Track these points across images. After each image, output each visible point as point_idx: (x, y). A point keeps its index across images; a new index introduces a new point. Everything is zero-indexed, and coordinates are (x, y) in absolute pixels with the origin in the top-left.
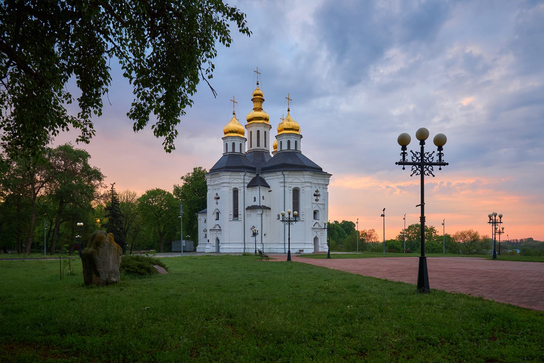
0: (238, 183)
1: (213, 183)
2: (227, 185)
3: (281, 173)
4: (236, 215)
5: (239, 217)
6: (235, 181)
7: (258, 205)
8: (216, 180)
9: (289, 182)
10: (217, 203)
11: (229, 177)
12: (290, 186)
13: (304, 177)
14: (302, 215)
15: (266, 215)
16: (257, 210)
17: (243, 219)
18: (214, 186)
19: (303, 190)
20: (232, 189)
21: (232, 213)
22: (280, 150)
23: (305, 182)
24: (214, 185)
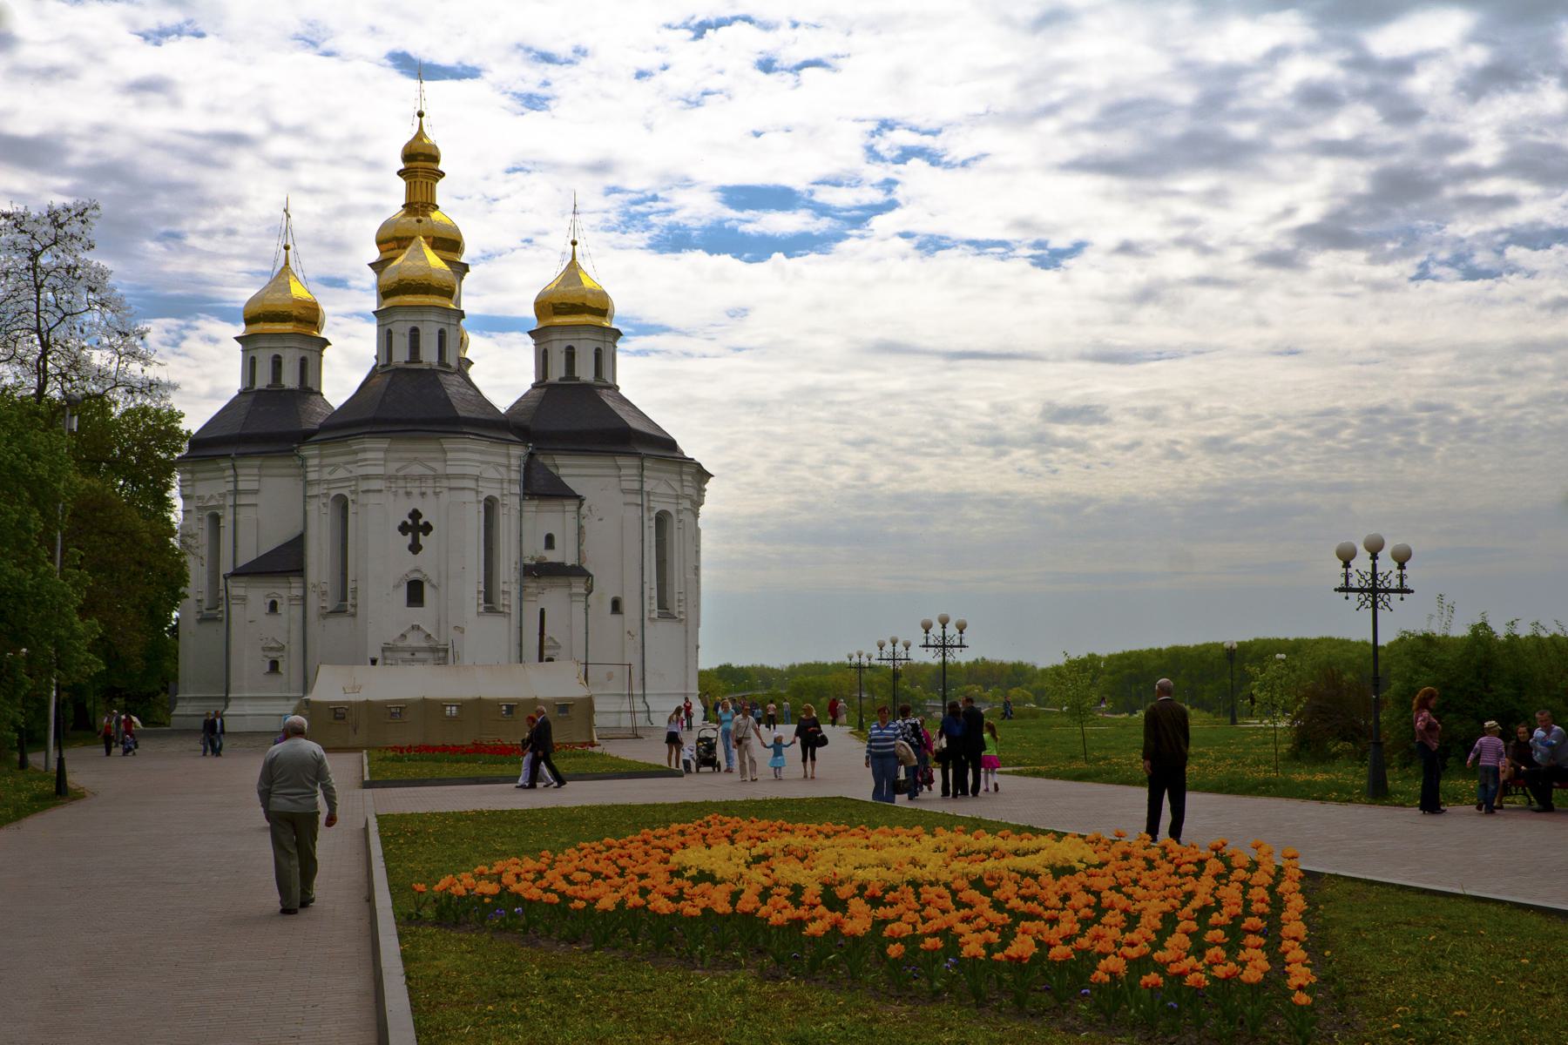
0: (501, 481)
1: (397, 470)
2: (471, 484)
3: (635, 462)
5: (501, 602)
6: (491, 473)
7: (570, 561)
9: (648, 494)
10: (415, 548)
12: (652, 504)
14: (679, 601)
15: (571, 595)
16: (572, 580)
17: (514, 610)
18: (401, 483)
19: (680, 521)
20: (483, 499)
21: (482, 588)
22: (563, 375)
24: (405, 478)
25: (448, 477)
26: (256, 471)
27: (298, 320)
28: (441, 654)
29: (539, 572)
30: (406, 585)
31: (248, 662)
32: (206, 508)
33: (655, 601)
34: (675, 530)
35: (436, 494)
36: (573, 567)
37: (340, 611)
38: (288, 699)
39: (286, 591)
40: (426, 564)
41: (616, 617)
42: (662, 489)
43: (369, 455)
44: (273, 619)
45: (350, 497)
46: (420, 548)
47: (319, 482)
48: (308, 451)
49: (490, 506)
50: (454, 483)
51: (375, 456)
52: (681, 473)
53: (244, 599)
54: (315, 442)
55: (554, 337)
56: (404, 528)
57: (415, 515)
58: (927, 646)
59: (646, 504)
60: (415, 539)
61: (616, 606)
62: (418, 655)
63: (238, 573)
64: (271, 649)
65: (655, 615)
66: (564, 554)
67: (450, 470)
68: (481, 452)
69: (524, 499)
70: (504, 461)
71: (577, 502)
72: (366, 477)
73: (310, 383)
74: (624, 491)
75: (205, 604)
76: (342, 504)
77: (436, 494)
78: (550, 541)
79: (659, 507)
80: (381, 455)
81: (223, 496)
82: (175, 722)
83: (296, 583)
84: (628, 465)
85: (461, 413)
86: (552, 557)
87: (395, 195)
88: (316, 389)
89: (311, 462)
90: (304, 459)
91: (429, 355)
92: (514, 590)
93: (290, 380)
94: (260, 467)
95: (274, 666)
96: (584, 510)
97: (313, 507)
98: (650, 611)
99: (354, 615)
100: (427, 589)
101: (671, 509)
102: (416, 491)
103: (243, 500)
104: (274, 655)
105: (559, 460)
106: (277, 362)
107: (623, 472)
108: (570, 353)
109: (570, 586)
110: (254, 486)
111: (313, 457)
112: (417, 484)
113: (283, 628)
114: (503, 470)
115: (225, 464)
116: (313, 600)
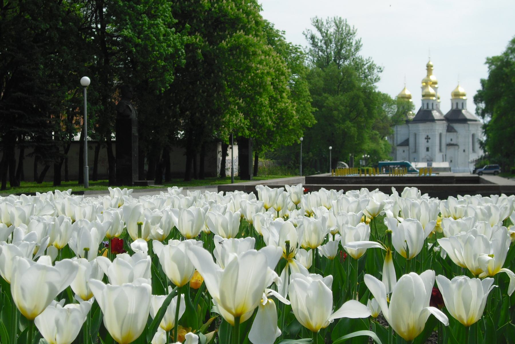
4: (440, 150)
7: (455, 143)
10: (428, 142)
29: (449, 145)
40: (429, 145)
49: (441, 135)
51: (422, 127)
56: (426, 138)
57: (428, 136)
61: (464, 151)
76: (415, 135)
78: (451, 140)
79: (472, 132)
83: (407, 147)
86: (452, 142)
87: (425, 72)
100: (430, 149)
103: (398, 132)
113: (406, 154)
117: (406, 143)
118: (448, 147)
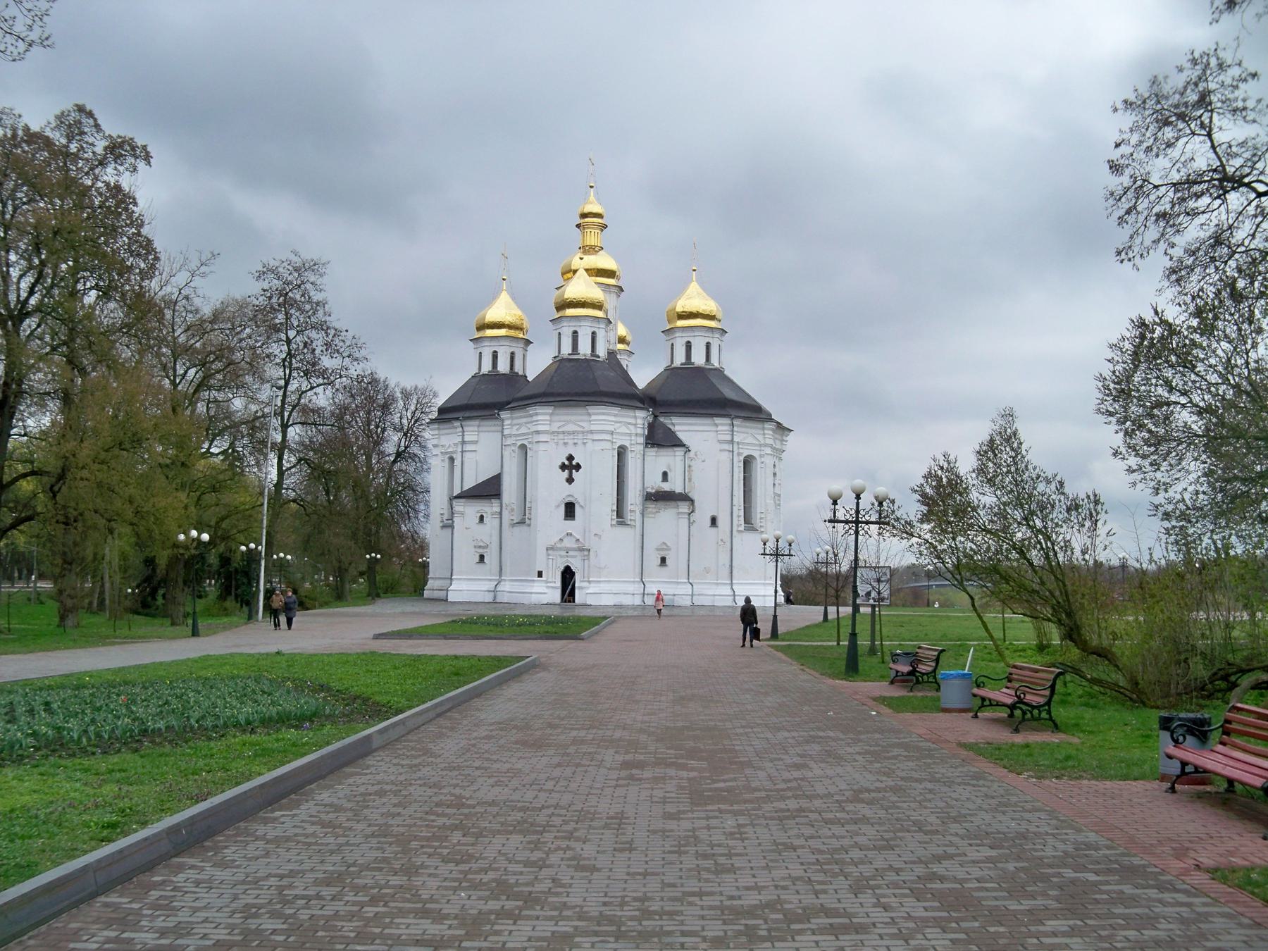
0: (630, 435)
2: (608, 437)
3: (727, 421)
6: (623, 430)
7: (679, 490)
8: (568, 422)
9: (738, 443)
10: (570, 480)
11: (612, 418)
12: (741, 451)
13: (764, 434)
16: (680, 503)
17: (638, 524)
18: (561, 436)
23: (766, 445)
24: (564, 433)
25: (592, 432)
26: (476, 429)
27: (510, 327)
28: (586, 553)
30: (563, 506)
31: (465, 555)
32: (447, 453)
33: (742, 519)
34: (759, 469)
35: (584, 443)
36: (680, 494)
37: (522, 522)
38: (490, 580)
39: (489, 508)
40: (575, 492)
41: (714, 529)
42: (750, 440)
43: (540, 418)
44: (481, 526)
45: (529, 446)
46: (573, 480)
47: (510, 436)
48: (505, 415)
49: (622, 453)
50: (596, 437)
52: (763, 429)
53: (462, 513)
54: (508, 409)
55: (677, 335)
56: (563, 467)
57: (570, 458)
58: (764, 554)
59: (735, 449)
60: (571, 474)
61: (714, 521)
62: (571, 553)
63: (458, 497)
64: (480, 547)
65: (742, 528)
66: (675, 485)
67: (593, 428)
68: (615, 415)
69: (646, 447)
70: (633, 421)
71: (683, 449)
72: (538, 432)
73: (518, 369)
74: (720, 442)
75: (446, 517)
77: (584, 443)
78: (665, 476)
79: (746, 453)
80: (548, 417)
81: (456, 445)
82: (427, 594)
83: (495, 502)
84: (723, 424)
85: (603, 388)
86: (666, 487)
88: (521, 373)
89: (507, 422)
90: (503, 420)
91: (584, 349)
92: (638, 509)
93: (503, 367)
94: (479, 426)
95: (482, 558)
96: (691, 454)
97: (507, 453)
98: (738, 526)
99: (529, 525)
100: (577, 509)
101: (756, 454)
102: (571, 442)
103: (468, 447)
104: (481, 551)
105: (675, 420)
106: (495, 356)
107: (720, 428)
108: (689, 346)
109: (678, 507)
110: (474, 438)
111: (508, 419)
112: (572, 437)
113: (488, 532)
114: (632, 427)
115: (457, 424)
116: (505, 513)
117: (489, 490)
118: (651, 507)
